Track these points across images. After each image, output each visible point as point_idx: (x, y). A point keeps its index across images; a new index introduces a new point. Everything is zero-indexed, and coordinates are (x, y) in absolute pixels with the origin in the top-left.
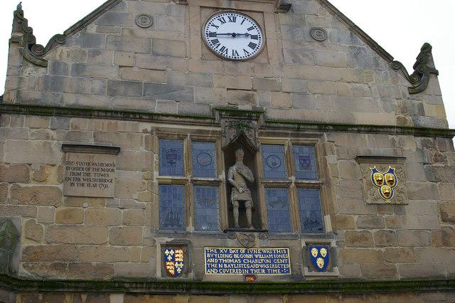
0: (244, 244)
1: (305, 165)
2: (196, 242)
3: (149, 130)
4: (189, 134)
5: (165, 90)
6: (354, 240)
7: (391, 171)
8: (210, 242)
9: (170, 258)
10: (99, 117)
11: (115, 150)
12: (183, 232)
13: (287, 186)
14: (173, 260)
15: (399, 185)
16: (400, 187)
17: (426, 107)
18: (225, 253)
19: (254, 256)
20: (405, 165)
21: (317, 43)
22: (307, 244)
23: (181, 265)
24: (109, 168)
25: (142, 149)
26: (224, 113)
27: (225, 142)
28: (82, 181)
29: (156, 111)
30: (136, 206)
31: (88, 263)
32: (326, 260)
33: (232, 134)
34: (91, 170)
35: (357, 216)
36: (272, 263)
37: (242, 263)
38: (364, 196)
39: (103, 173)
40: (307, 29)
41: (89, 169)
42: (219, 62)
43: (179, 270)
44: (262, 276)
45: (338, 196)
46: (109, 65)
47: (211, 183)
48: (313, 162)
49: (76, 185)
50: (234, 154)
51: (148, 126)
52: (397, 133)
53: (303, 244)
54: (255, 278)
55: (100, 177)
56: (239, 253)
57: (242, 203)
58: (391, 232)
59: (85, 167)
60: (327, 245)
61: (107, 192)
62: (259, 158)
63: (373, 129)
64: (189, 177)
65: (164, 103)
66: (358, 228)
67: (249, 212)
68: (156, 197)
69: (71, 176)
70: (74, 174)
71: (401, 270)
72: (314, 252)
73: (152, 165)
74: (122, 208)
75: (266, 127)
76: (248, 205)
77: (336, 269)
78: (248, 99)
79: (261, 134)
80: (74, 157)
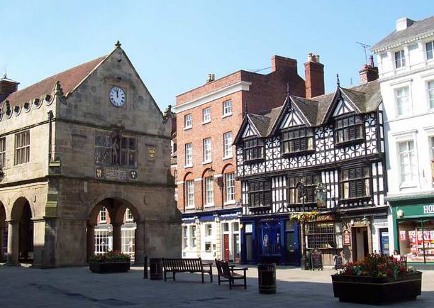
5: (98, 117)
6: (143, 170)
17: (166, 128)
21: (140, 103)
33: (116, 134)
40: (138, 96)
42: (113, 108)
46: (85, 106)
51: (94, 129)
63: (153, 136)
71: (152, 180)
80: (76, 139)
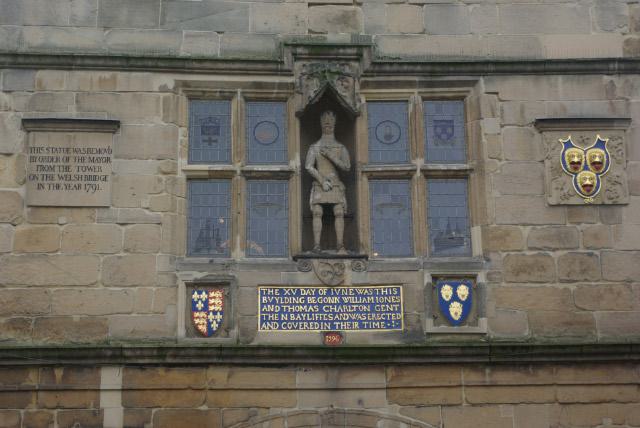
0: (326, 279)
1: (444, 136)
2: (242, 276)
3: (171, 84)
4: (239, 91)
7: (600, 144)
8: (268, 277)
9: (200, 305)
10: (83, 67)
11: (111, 126)
12: (224, 260)
13: (408, 176)
14: (205, 309)
15: (614, 170)
16: (615, 174)
18: (292, 295)
19: (341, 300)
20: (628, 131)
22: (435, 278)
23: (219, 317)
24: (100, 156)
25: (159, 121)
26: (299, 50)
27: (298, 103)
28: (57, 181)
29: (182, 54)
30: (147, 221)
31: (66, 317)
32: (467, 305)
33: (313, 88)
34: (72, 160)
35: (529, 228)
36: (372, 311)
37: (321, 311)
38: (545, 192)
39: (91, 165)
41: (68, 159)
43: (214, 326)
44: (354, 335)
45: (496, 193)
47: (275, 175)
48: (458, 132)
49: (46, 187)
50: (319, 124)
51: (169, 80)
52: (621, 72)
53: (428, 279)
54: (340, 335)
55: (88, 173)
56: (317, 295)
57: (328, 209)
58: (590, 255)
59: (61, 155)
60: (470, 280)
61: (97, 199)
62: (361, 127)
64: (237, 167)
65: (193, 36)
66: (531, 249)
67: (339, 224)
68: (182, 203)
69: (38, 173)
70: (43, 168)
72: (446, 292)
73: (174, 149)
74: (122, 224)
75: (372, 72)
76: (339, 210)
77: (483, 321)
78: (345, 20)
79: (364, 85)
80: (43, 140)
